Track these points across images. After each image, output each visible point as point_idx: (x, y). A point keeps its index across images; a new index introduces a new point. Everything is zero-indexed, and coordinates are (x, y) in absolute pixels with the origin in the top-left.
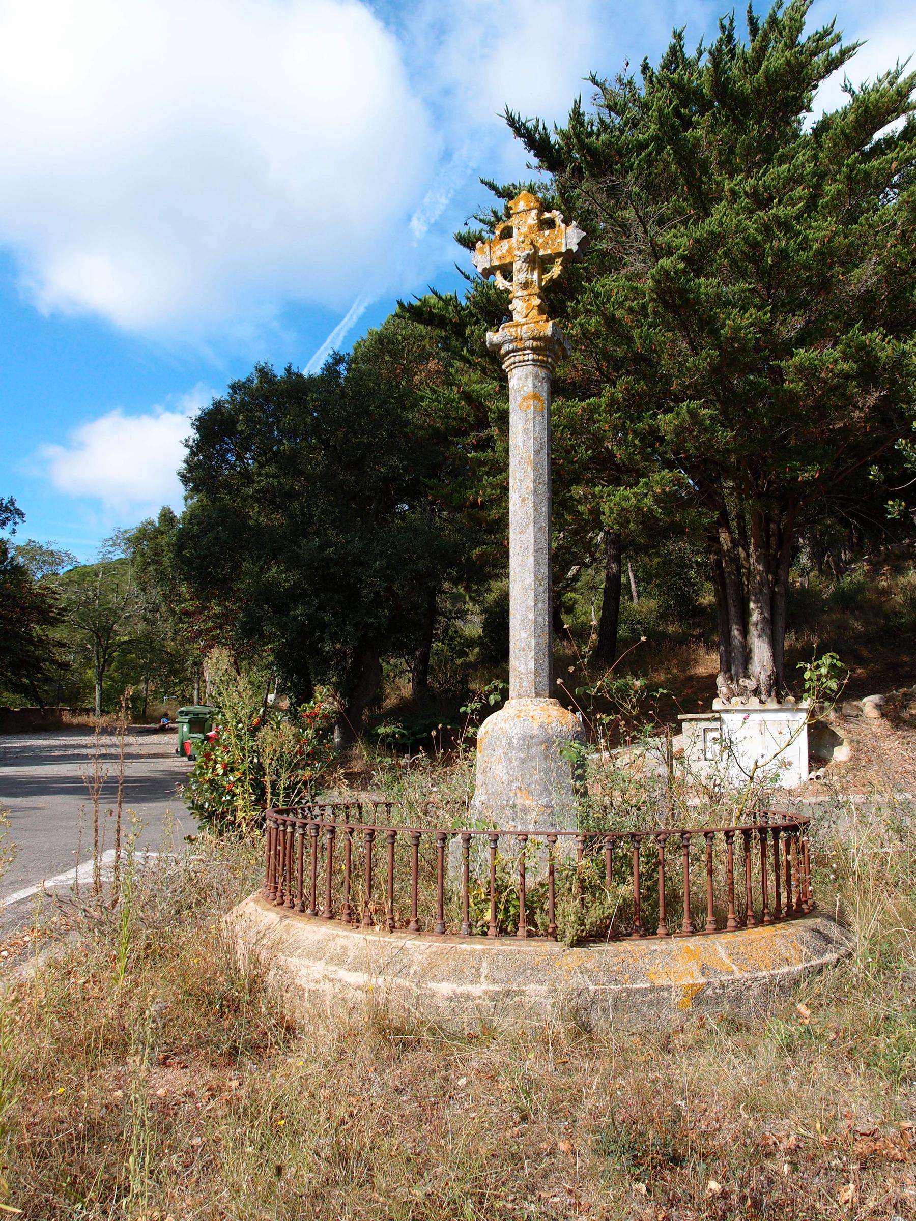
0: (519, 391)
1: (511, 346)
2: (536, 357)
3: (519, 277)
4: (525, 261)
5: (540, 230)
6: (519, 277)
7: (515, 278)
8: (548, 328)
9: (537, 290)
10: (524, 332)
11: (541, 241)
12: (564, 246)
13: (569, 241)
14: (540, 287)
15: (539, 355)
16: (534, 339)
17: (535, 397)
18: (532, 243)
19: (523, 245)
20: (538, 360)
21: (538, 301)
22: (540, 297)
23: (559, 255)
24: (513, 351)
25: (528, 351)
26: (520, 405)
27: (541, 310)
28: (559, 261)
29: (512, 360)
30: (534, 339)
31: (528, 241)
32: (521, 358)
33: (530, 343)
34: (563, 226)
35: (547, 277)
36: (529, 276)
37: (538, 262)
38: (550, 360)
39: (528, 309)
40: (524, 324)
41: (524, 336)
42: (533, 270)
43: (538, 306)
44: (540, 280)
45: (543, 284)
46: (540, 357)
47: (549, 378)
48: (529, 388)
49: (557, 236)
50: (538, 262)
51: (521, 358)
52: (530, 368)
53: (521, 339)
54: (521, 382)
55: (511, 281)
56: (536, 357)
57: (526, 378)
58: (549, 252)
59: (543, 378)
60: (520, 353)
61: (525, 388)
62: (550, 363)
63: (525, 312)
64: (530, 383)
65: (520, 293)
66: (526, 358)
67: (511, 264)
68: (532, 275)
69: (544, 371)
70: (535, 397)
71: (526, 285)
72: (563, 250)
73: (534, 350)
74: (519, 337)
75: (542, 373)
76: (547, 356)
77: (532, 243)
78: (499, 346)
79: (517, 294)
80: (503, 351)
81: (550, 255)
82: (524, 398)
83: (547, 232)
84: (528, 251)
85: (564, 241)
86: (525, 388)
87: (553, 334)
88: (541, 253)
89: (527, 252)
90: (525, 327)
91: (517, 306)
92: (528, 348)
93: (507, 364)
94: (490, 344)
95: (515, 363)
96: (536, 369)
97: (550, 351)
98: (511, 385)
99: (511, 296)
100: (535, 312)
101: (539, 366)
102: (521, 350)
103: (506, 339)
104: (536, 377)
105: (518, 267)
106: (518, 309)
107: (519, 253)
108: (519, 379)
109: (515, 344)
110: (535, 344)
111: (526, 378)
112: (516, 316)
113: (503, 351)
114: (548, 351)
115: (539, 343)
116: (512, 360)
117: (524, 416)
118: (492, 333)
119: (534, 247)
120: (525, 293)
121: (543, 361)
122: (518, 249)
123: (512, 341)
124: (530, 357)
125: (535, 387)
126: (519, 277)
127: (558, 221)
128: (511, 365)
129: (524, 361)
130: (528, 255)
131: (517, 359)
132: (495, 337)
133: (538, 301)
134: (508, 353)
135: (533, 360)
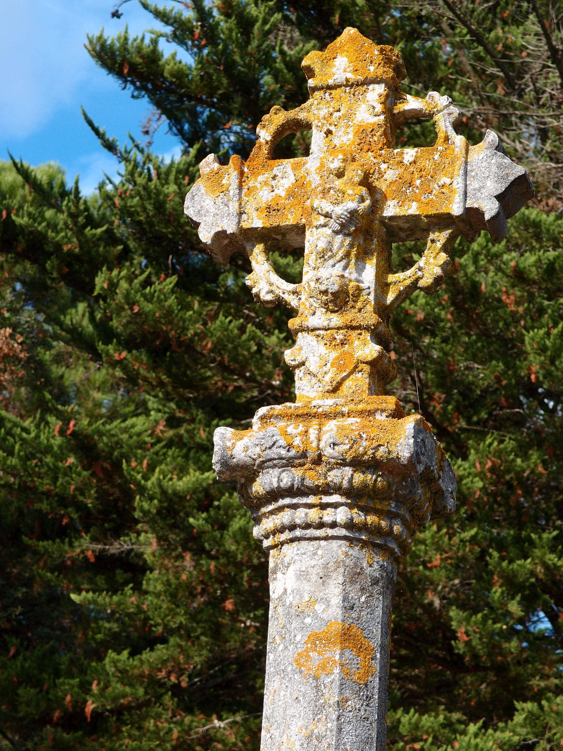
0: (300, 614)
1: (287, 478)
2: (359, 517)
3: (324, 273)
4: (343, 230)
5: (389, 145)
6: (324, 273)
7: (308, 275)
8: (402, 438)
9: (370, 317)
10: (329, 438)
11: (391, 175)
12: (458, 198)
13: (473, 185)
14: (381, 309)
15: (366, 510)
16: (357, 463)
17: (348, 637)
18: (366, 182)
19: (338, 183)
20: (364, 528)
21: (372, 350)
22: (378, 338)
23: (442, 221)
24: (290, 492)
25: (336, 498)
26: (300, 661)
27: (381, 376)
28: (441, 237)
29: (285, 517)
30: (357, 463)
31: (354, 173)
32: (314, 515)
33: (342, 476)
34: (459, 140)
35: (400, 279)
36: (351, 274)
37: (381, 236)
38: (397, 528)
39: (340, 368)
40: (327, 416)
41: (328, 452)
42: (363, 255)
43: (372, 364)
44: (382, 286)
45: (390, 297)
46: (371, 519)
47: (390, 581)
48: (330, 607)
49: (438, 168)
50: (381, 236)
51: (314, 515)
52: (338, 549)
53: (318, 461)
54: (307, 587)
55: (294, 278)
56: (359, 517)
57: (324, 578)
58: (413, 209)
59: (375, 582)
60: (311, 499)
61: (319, 608)
62: (397, 538)
63: (330, 376)
64: (334, 592)
65: (320, 319)
66: (328, 516)
67: (300, 230)
68: (360, 270)
69: (379, 559)
70: (348, 637)
71: (339, 300)
72: (456, 210)
73: (355, 496)
74: (312, 454)
75: (373, 564)
76: (391, 516)
77: (366, 182)
78: (250, 472)
79: (313, 322)
80: (259, 487)
81: (415, 218)
82: (316, 640)
83: (410, 153)
84: (352, 202)
85: (458, 184)
86: (319, 608)
87: (416, 457)
88: (391, 210)
89: (352, 205)
90: (331, 425)
91: (311, 356)
92: (338, 489)
93: (268, 524)
94: (225, 463)
95: (292, 527)
96: (355, 551)
97: (400, 500)
98: (276, 588)
99: (293, 323)
100: (361, 380)
101: (364, 544)
102: (316, 491)
103: (273, 453)
104: (354, 576)
105: (322, 245)
106: (313, 365)
107: (326, 207)
108: (302, 575)
109: (297, 473)
110: (359, 478)
111: (324, 578)
112: (305, 389)
113: (259, 487)
114: (390, 500)
115: (370, 478)
116: (285, 517)
117: (311, 694)
118: (229, 431)
119: (372, 190)
120: (336, 320)
121: (376, 531)
122: (325, 192)
123: (289, 463)
124: (342, 515)
125: (349, 607)
126: (322, 270)
127: (444, 124)
128: (281, 530)
129: (321, 525)
130: (353, 213)
131: (300, 516)
132: (240, 445)
133: (372, 350)
134: (274, 495)
135: (350, 525)
